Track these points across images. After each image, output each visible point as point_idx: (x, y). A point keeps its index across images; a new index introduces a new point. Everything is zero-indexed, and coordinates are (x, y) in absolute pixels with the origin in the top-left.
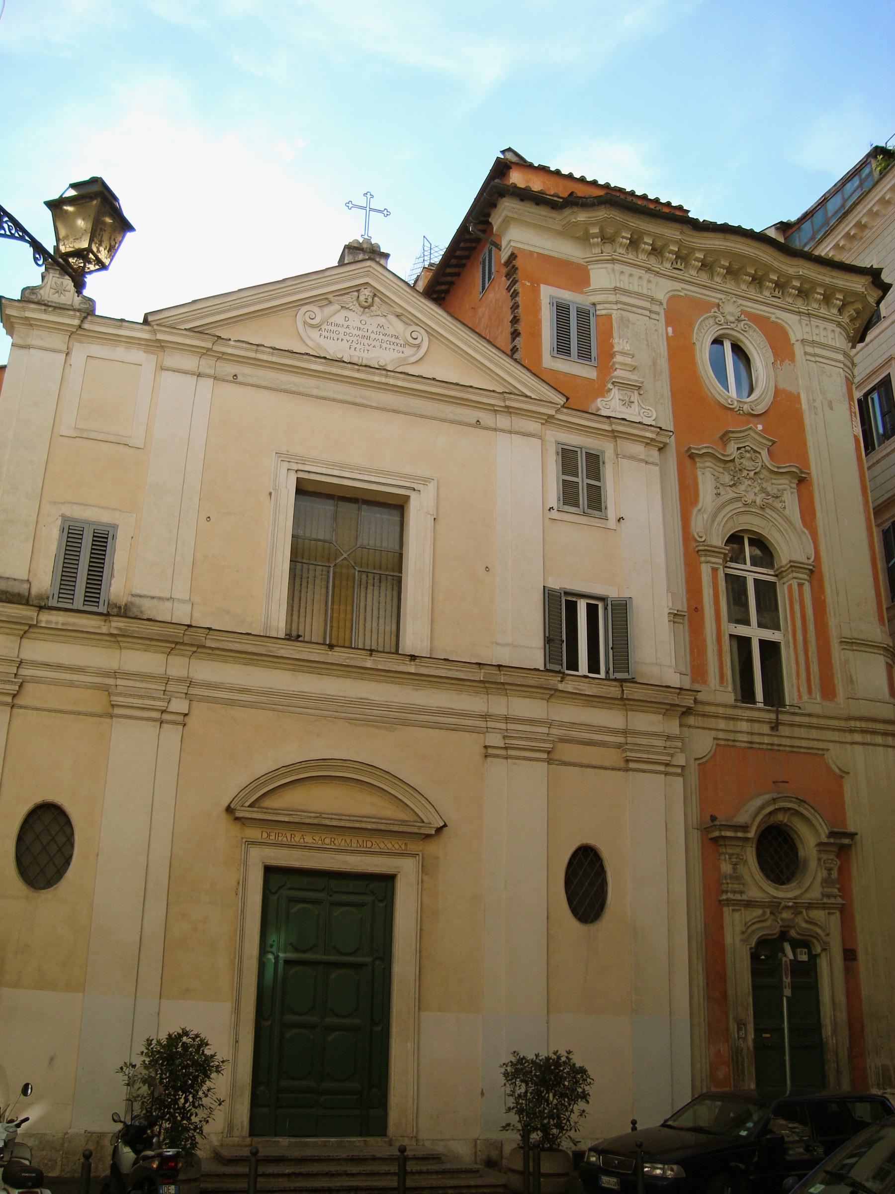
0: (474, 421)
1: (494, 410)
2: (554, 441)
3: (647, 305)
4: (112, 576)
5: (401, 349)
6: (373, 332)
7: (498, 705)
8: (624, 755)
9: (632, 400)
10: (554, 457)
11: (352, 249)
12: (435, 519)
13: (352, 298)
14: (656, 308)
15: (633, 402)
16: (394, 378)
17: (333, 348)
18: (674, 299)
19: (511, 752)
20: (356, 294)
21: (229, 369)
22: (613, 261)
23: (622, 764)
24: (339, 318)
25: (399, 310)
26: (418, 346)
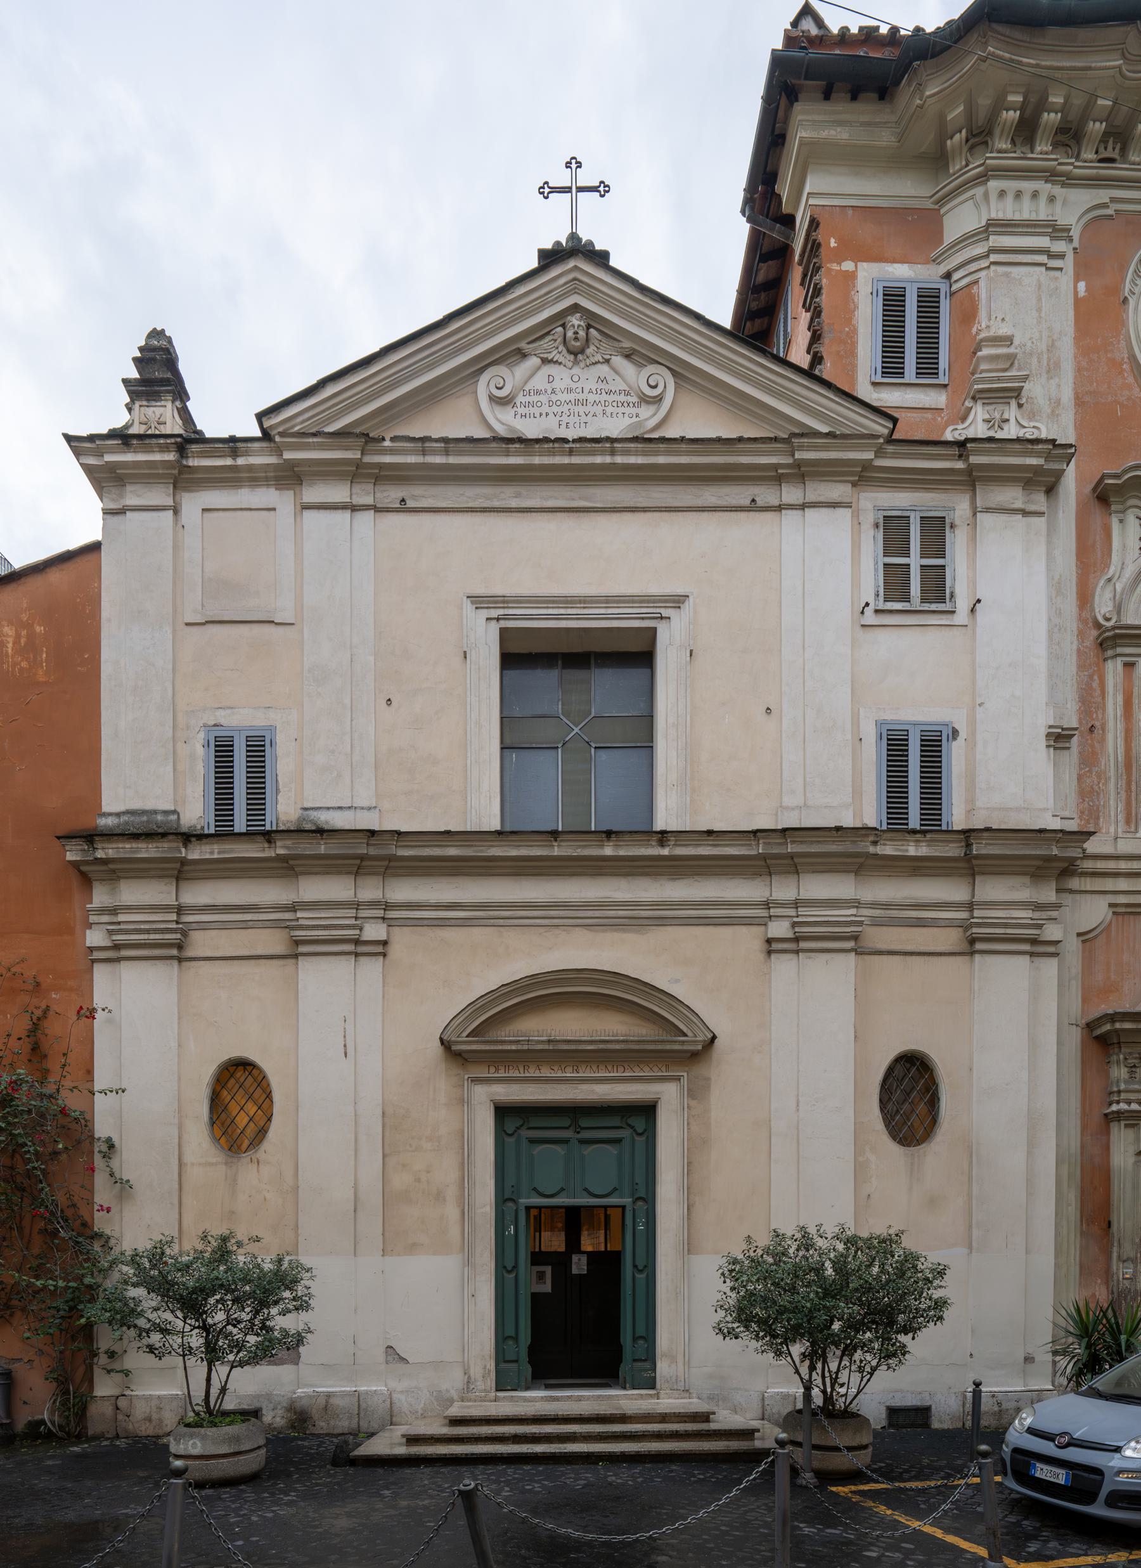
0: (747, 502)
1: (775, 477)
2: (870, 506)
3: (1043, 242)
4: (278, 791)
5: (634, 411)
6: (590, 391)
7: (784, 890)
8: (969, 933)
9: (1006, 416)
10: (872, 532)
11: (550, 258)
12: (691, 652)
13: (556, 340)
14: (1059, 246)
15: (1008, 420)
16: (626, 452)
17: (531, 429)
18: (1096, 221)
19: (803, 945)
20: (560, 329)
21: (391, 494)
22: (983, 178)
23: (965, 947)
24: (539, 382)
25: (627, 344)
26: (658, 400)
